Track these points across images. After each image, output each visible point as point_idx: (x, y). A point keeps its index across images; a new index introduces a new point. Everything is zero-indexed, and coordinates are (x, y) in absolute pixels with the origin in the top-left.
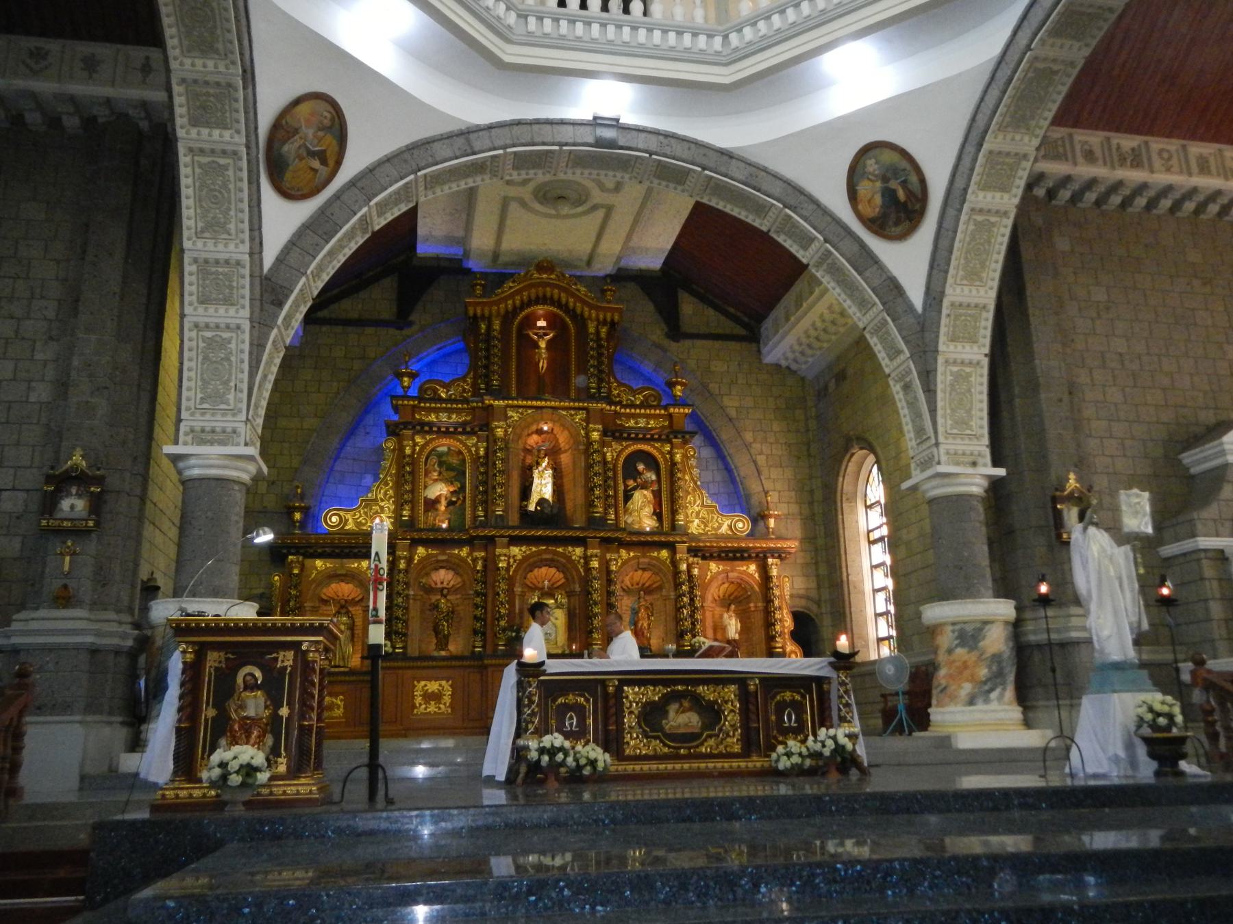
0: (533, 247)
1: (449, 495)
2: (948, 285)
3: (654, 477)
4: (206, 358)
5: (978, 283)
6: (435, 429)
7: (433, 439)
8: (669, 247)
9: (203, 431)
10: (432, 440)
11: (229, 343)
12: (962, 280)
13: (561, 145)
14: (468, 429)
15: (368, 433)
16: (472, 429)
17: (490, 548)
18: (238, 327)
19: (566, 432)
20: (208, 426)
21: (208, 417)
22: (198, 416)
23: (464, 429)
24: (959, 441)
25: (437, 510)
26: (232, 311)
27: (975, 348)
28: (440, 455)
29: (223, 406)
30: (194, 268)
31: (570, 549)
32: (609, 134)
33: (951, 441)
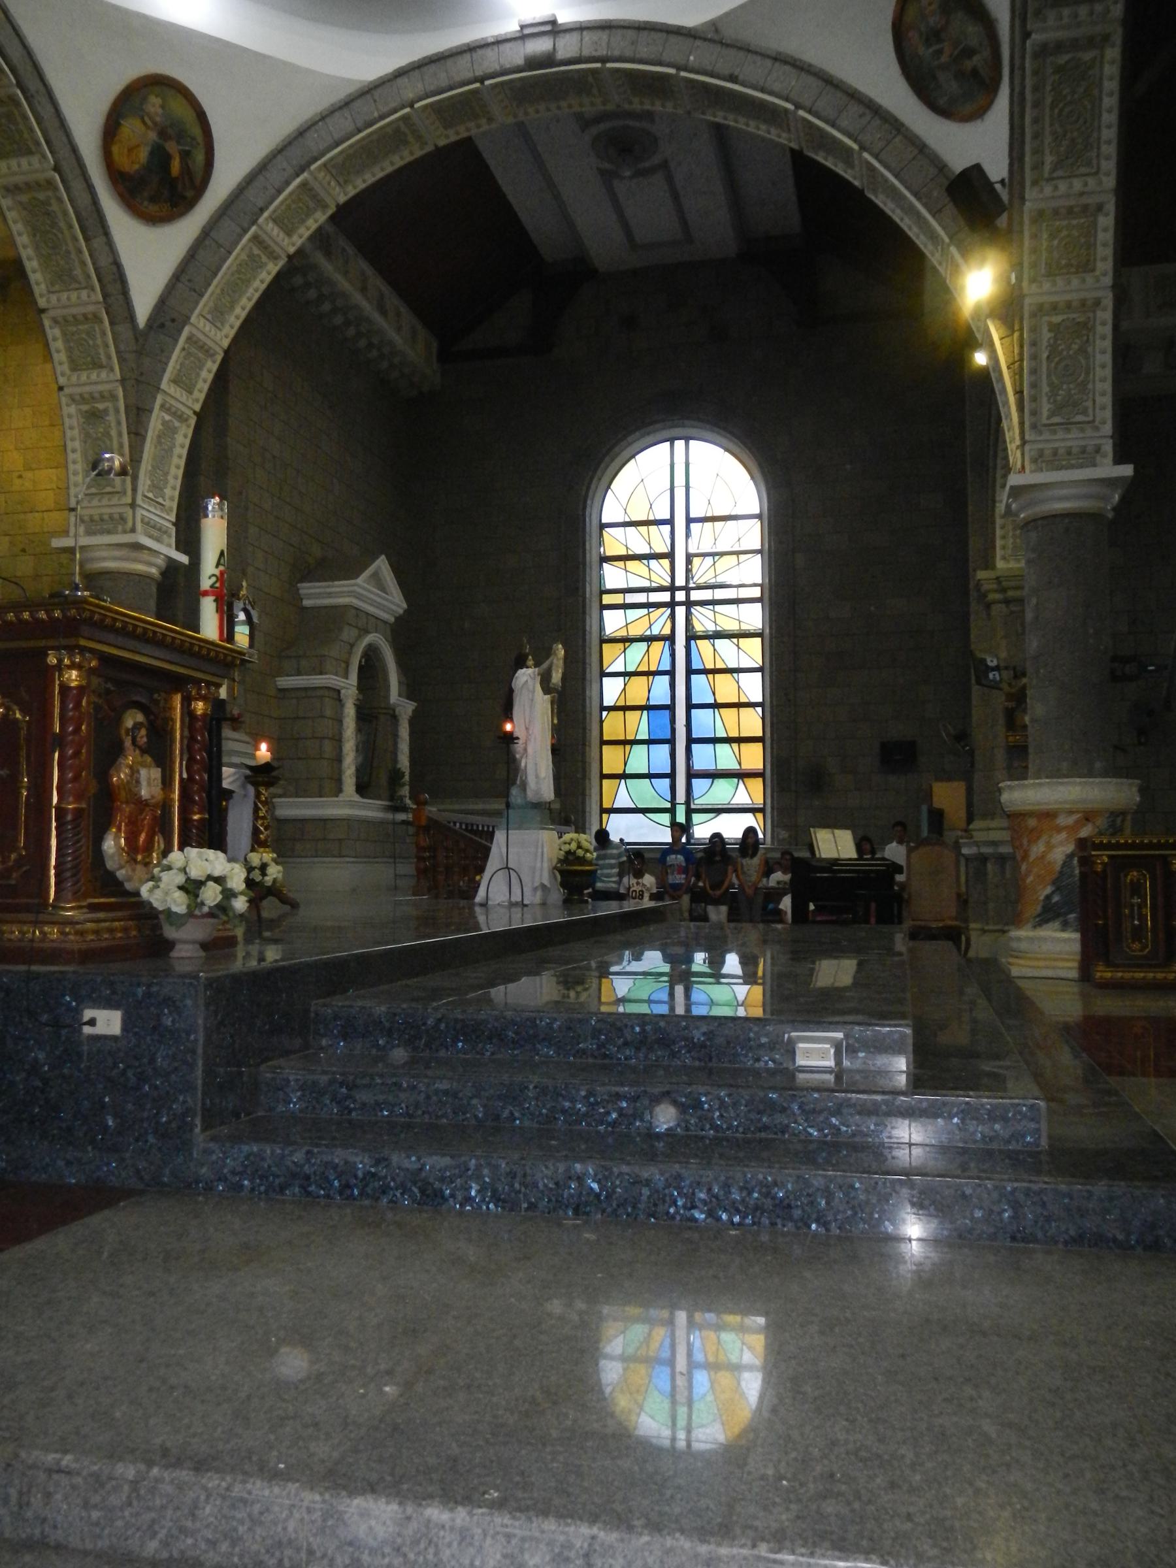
2: (1028, 183)
4: (87, 435)
5: (1083, 170)
9: (92, 520)
11: (107, 415)
12: (1053, 170)
13: (481, 80)
18: (114, 397)
20: (95, 512)
21: (95, 502)
22: (85, 504)
24: (1060, 435)
26: (104, 375)
27: (1090, 279)
29: (109, 489)
30: (57, 332)
32: (541, 46)
33: (1046, 436)
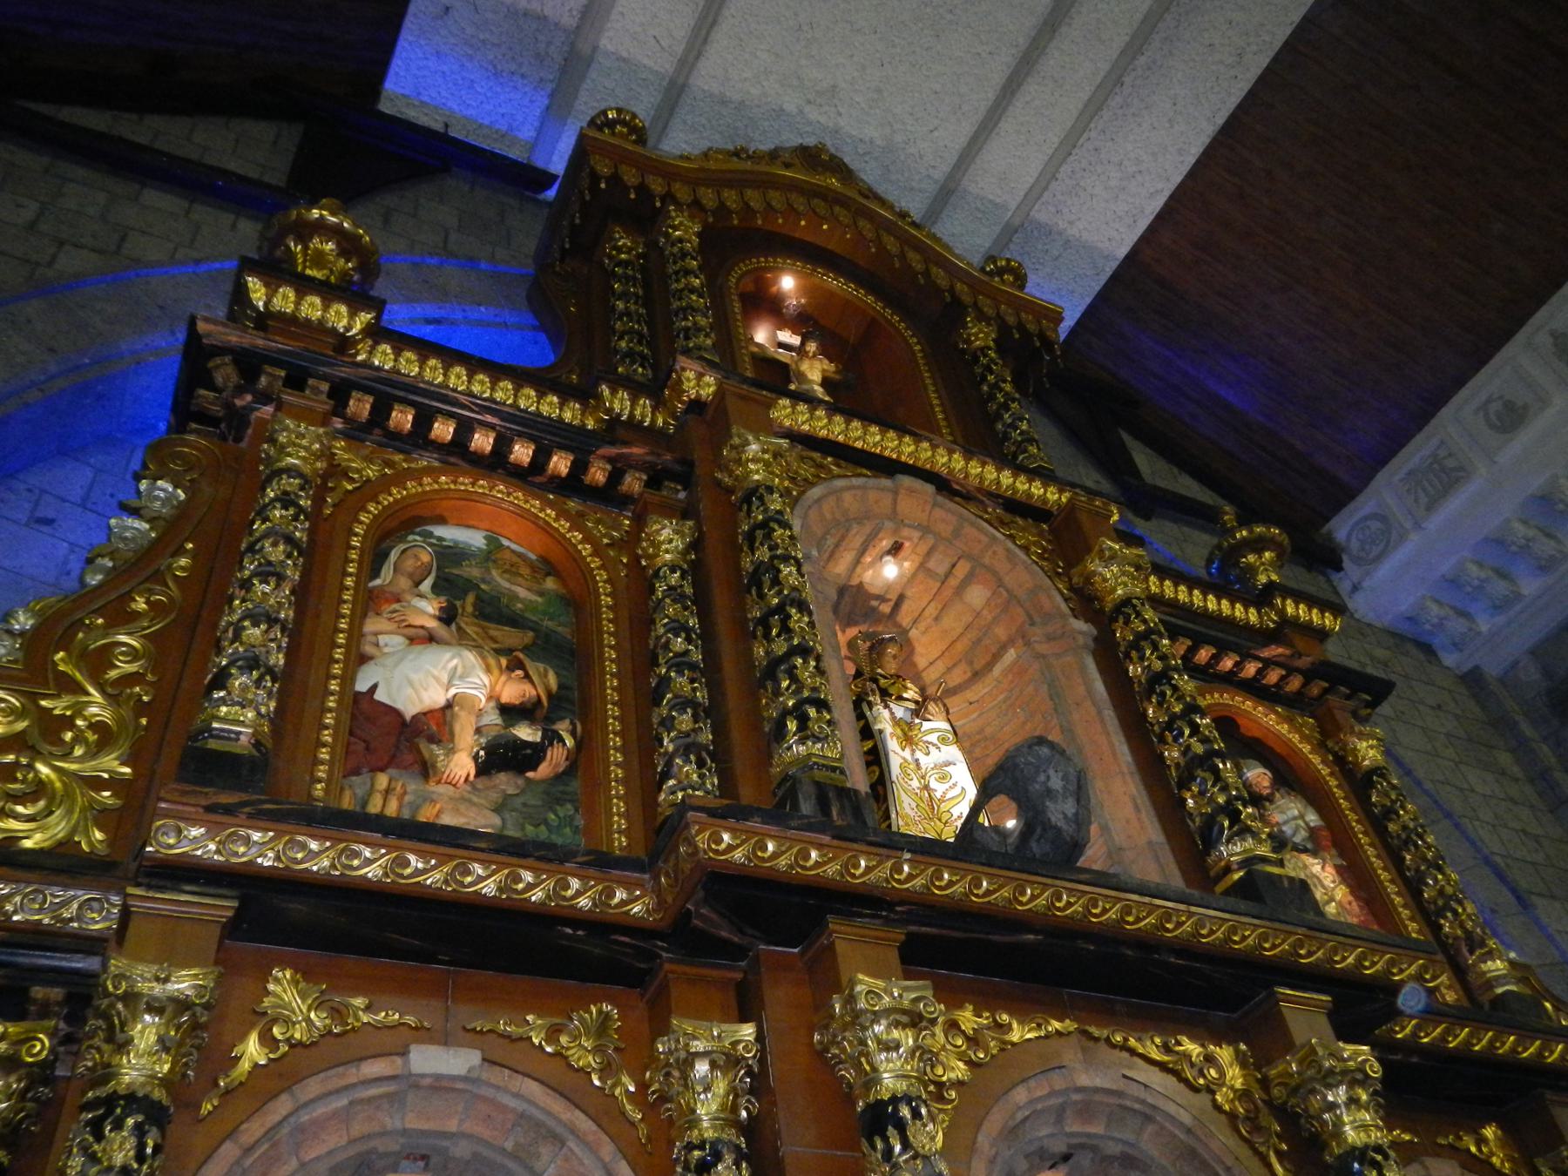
0: (791, 103)
1: (493, 718)
3: (1313, 818)
6: (443, 430)
7: (428, 471)
8: (1122, 252)
10: (417, 475)
14: (598, 474)
15: (49, 522)
16: (615, 477)
17: (779, 996)
19: (977, 595)
23: (579, 467)
25: (426, 770)
28: (449, 555)
31: (1192, 1048)
